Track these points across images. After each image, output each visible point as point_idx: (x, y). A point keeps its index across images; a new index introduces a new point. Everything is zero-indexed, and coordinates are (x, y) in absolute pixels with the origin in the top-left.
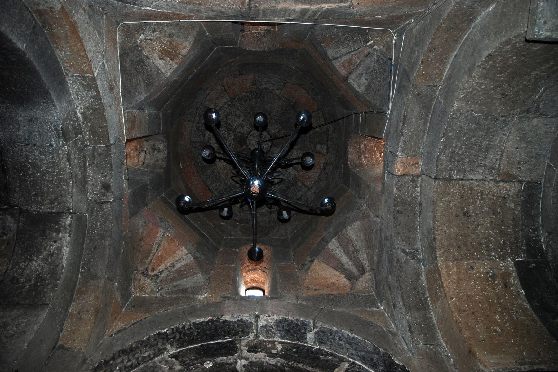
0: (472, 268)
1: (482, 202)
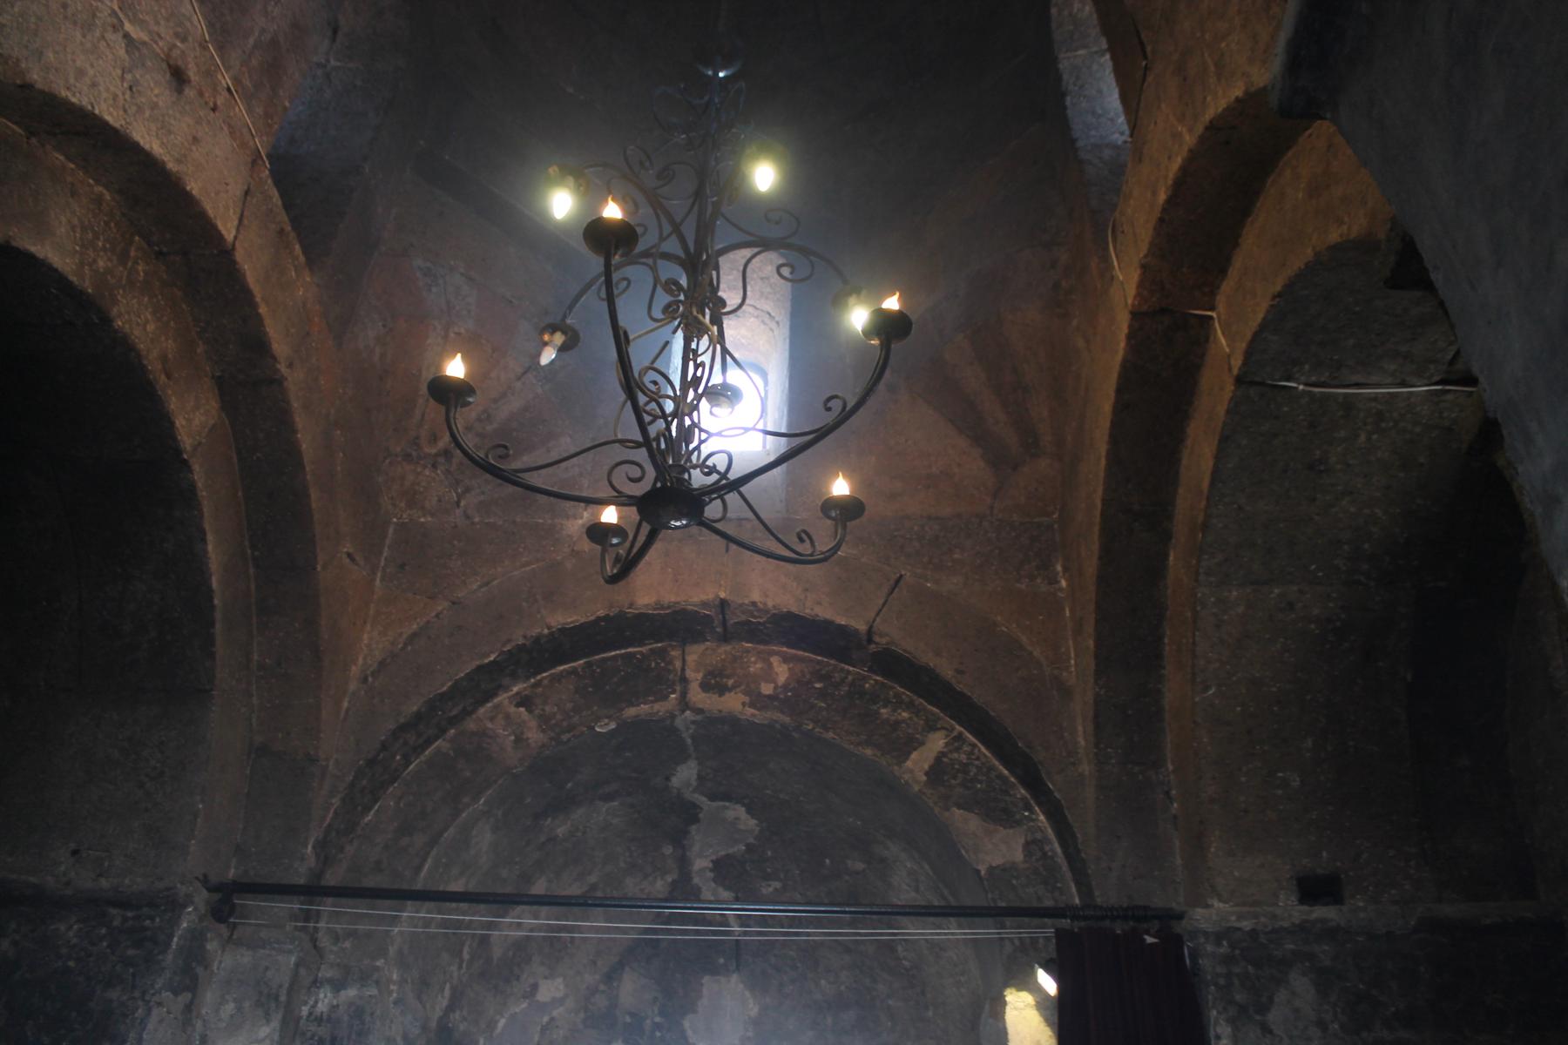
0: (1291, 606)
1: (1375, 437)
